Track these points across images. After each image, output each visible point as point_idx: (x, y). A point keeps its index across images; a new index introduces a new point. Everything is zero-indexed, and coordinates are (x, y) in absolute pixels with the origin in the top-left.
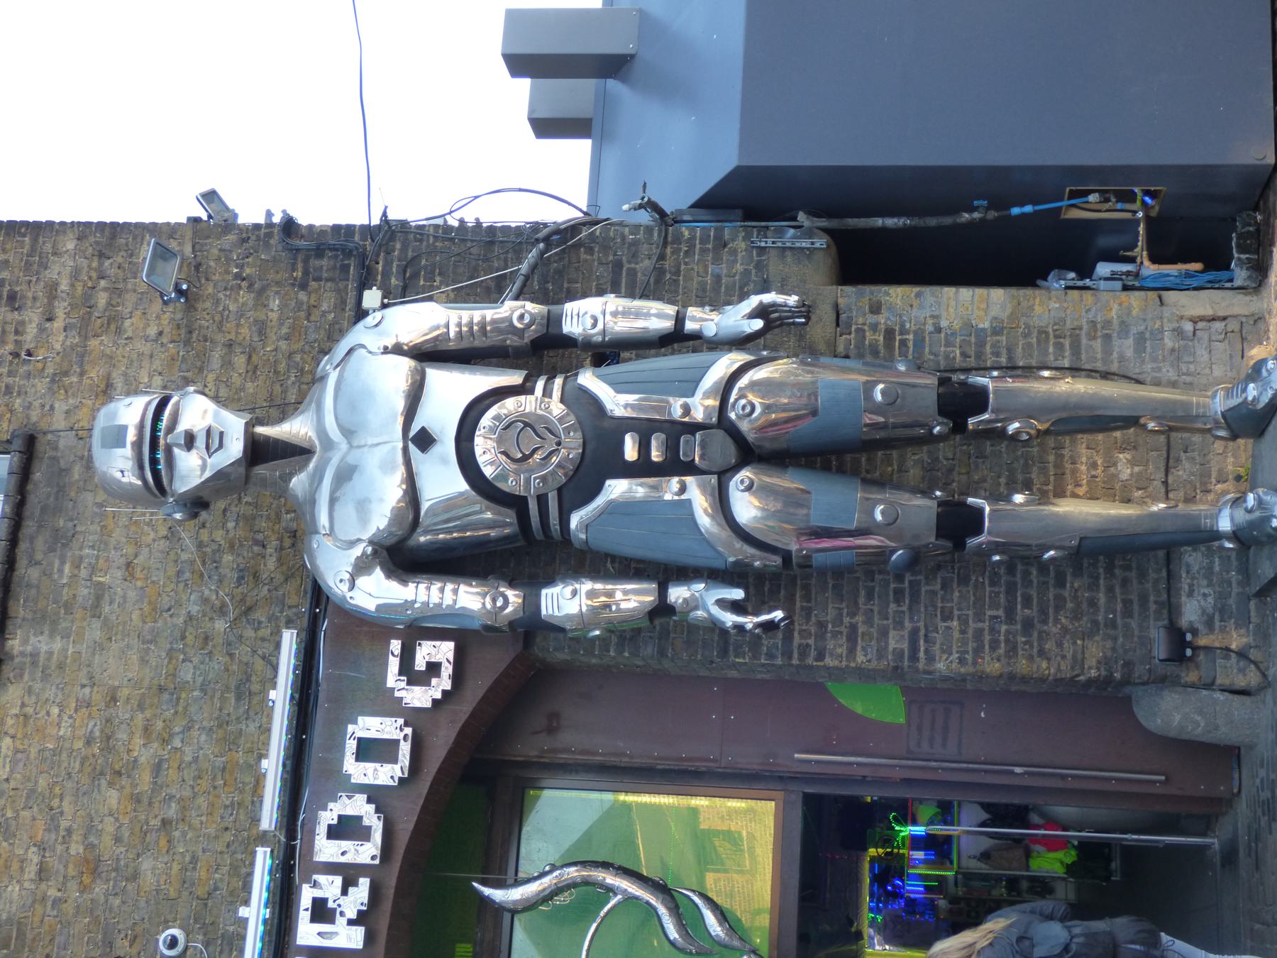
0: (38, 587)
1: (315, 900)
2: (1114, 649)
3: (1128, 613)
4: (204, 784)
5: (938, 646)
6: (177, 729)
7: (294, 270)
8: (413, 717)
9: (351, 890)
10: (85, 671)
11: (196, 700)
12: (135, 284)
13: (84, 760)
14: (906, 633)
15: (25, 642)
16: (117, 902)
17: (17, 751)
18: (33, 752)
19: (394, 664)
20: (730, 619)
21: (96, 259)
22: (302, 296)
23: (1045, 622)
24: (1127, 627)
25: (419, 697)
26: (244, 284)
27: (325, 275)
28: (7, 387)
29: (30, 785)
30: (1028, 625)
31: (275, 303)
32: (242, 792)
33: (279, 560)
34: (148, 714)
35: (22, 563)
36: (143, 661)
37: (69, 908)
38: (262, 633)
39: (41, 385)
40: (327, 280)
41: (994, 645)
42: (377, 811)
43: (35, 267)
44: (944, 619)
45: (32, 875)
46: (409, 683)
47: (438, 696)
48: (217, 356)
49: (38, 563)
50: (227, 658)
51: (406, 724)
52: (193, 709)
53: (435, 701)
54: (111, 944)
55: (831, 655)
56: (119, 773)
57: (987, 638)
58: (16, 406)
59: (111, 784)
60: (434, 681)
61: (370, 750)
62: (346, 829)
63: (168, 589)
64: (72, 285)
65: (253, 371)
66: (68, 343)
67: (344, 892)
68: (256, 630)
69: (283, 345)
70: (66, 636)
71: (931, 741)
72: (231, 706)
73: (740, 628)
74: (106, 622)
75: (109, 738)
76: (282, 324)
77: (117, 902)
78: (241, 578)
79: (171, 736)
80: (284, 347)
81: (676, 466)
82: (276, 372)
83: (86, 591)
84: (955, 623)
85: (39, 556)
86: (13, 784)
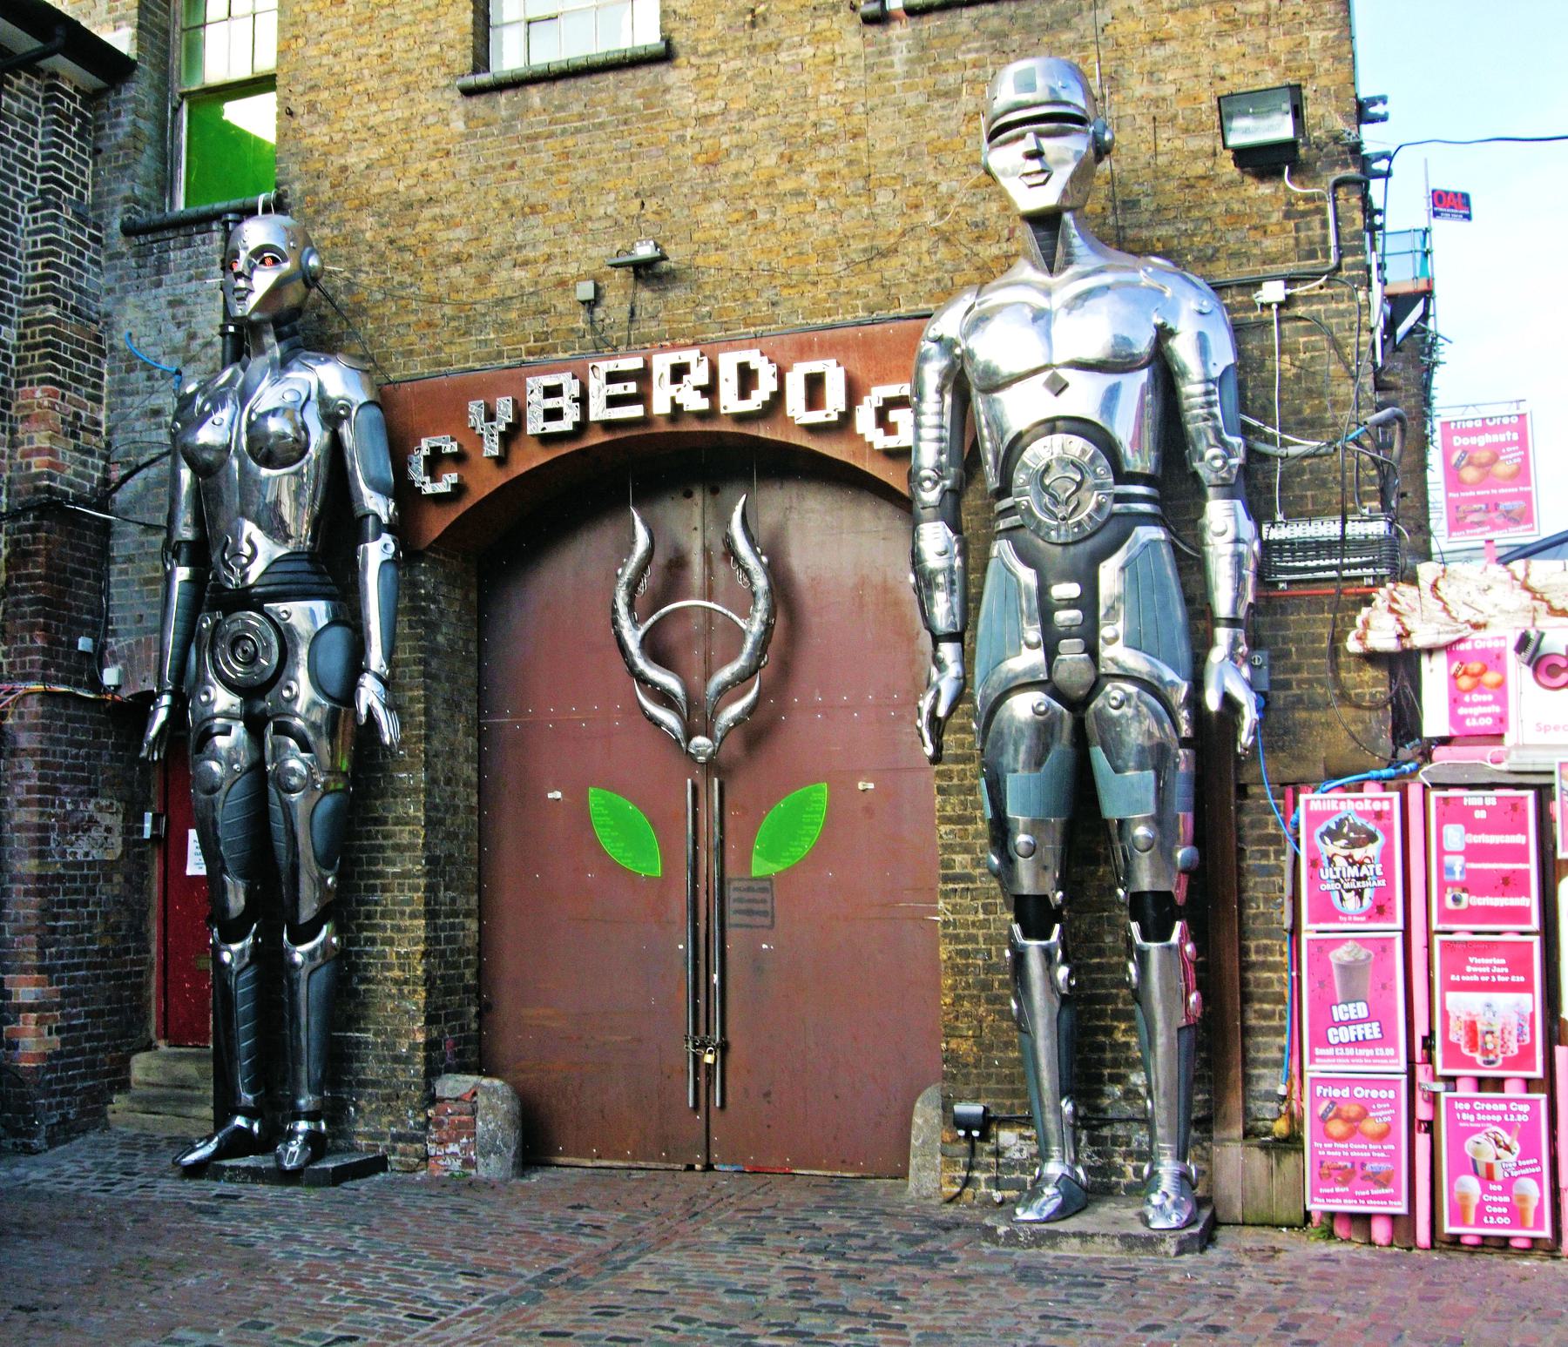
2: (966, 1065)
4: (787, 239)
8: (847, 418)
10: (877, 101)
14: (969, 870)
15: (900, 39)
16: (685, 190)
19: (893, 391)
20: (925, 704)
22: (1276, 216)
23: (989, 1001)
25: (865, 420)
27: (1302, 235)
29: (775, 84)
33: (997, 257)
34: (845, 171)
36: (891, 154)
37: (678, 150)
38: (926, 258)
40: (1297, 239)
42: (764, 403)
44: (985, 906)
45: (702, 111)
47: (867, 439)
50: (899, 230)
52: (851, 212)
54: (653, 194)
55: (944, 801)
57: (970, 947)
59: (782, 156)
61: (815, 384)
62: (747, 378)
67: (696, 388)
69: (1220, 208)
70: (908, 75)
71: (740, 900)
72: (857, 245)
73: (920, 716)
74: (923, 108)
75: (820, 142)
77: (685, 190)
79: (827, 198)
80: (1217, 211)
82: (1189, 209)
83: (951, 81)
84: (981, 916)
86: (774, 68)
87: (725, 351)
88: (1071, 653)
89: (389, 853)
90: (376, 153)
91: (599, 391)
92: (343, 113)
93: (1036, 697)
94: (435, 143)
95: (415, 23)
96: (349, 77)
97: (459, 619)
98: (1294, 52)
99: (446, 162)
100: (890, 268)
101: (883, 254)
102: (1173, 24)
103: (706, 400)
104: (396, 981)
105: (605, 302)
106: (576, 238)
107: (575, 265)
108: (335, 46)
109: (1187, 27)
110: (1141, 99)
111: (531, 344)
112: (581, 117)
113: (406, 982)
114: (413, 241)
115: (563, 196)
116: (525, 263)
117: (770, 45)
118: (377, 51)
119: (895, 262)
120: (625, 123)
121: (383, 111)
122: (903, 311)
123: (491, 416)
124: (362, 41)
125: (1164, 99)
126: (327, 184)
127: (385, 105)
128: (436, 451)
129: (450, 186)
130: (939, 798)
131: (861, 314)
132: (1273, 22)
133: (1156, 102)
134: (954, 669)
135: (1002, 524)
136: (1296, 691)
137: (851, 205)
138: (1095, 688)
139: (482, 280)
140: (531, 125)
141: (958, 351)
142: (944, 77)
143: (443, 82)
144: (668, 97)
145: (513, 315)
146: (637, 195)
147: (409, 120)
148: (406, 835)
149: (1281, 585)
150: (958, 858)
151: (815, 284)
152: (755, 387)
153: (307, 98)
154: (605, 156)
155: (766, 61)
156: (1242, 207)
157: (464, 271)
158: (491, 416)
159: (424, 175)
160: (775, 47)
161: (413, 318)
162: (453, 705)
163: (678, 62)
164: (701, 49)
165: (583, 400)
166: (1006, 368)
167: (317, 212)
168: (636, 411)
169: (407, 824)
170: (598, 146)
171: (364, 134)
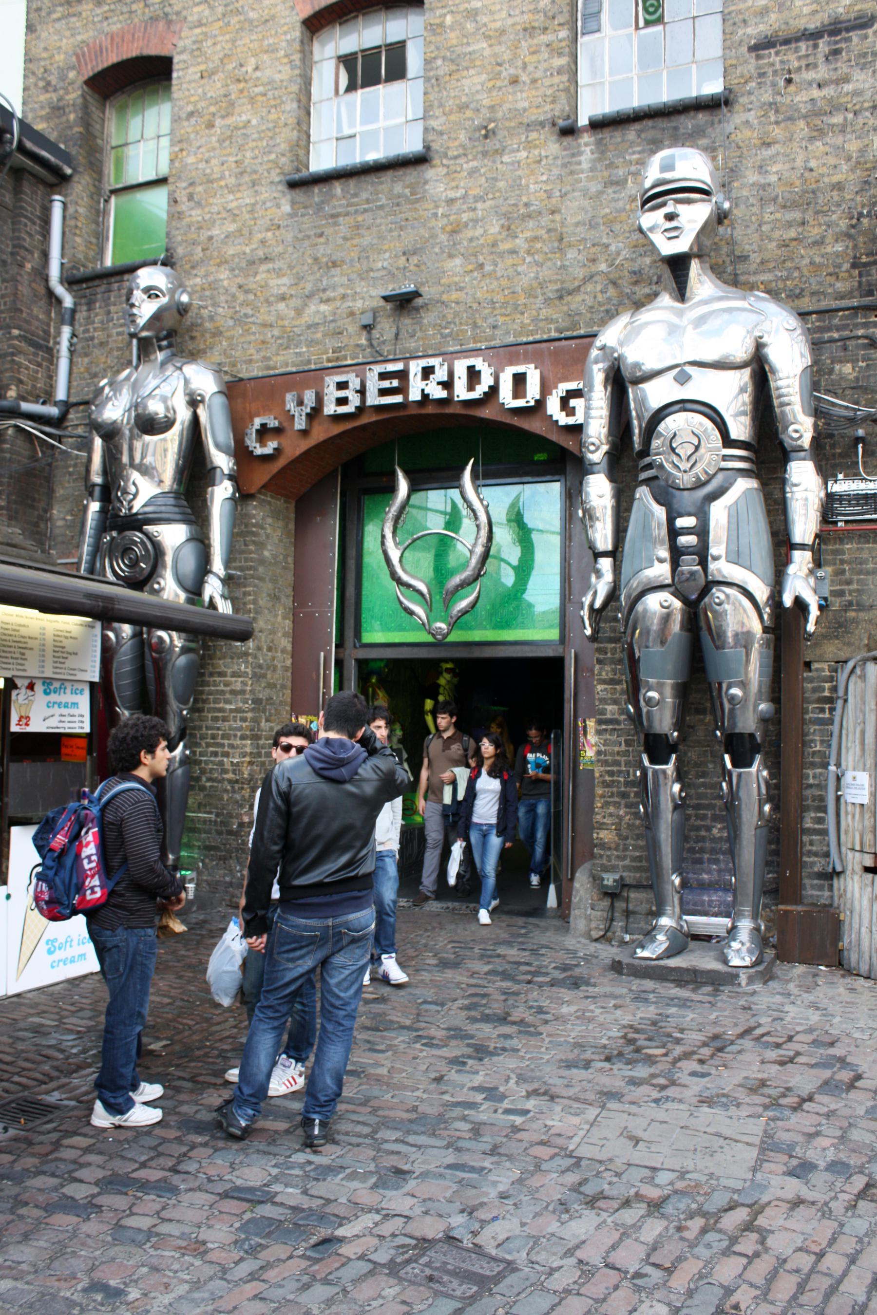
0: (623, 141)
1: (433, 367)
3: (634, 859)
4: (504, 282)
5: (608, 737)
6: (536, 257)
7: (867, 255)
8: (540, 404)
9: (440, 387)
10: (569, 188)
11: (555, 264)
12: (850, 140)
13: (515, 205)
14: (616, 716)
15: (586, 145)
17: (519, 162)
18: (519, 173)
19: (573, 385)
20: (587, 600)
21: (871, 104)
22: (846, 266)
23: (626, 806)
24: (624, 858)
25: (553, 406)
26: (854, 221)
27: (864, 279)
28: (764, 73)
29: (500, 177)
30: (624, 795)
31: (839, 247)
32: (501, 307)
34: (545, 236)
35: (637, 126)
36: (577, 224)
37: (433, 223)
38: (599, 295)
39: (767, 96)
40: (860, 283)
41: (611, 773)
42: (485, 393)
43: (863, 61)
44: (626, 741)
46: (562, 398)
47: (555, 418)
48: (796, 215)
49: (639, 136)
51: (536, 401)
52: (549, 264)
53: (551, 416)
54: (414, 253)
55: (601, 669)
56: (509, 229)
57: (615, 769)
58: (750, 84)
59: (502, 226)
60: (564, 413)
61: (519, 380)
63: (625, 227)
64: (848, 94)
65: (784, 244)
66: (801, 105)
67: (439, 383)
68: (601, 292)
69: (806, 261)
70: (592, 170)
73: (582, 608)
74: (601, 193)
75: (529, 216)
76: (823, 256)
77: (437, 250)
78: (635, 273)
80: (804, 262)
81: (676, 554)
82: (784, 261)
83: (621, 173)
85: (643, 136)
86: (499, 166)
87: (459, 358)
88: (689, 564)
89: (228, 696)
90: (232, 227)
91: (373, 385)
92: (211, 200)
93: (665, 596)
94: (271, 220)
95: (261, 139)
96: (215, 176)
97: (281, 541)
98: (862, 151)
99: (277, 233)
100: (576, 302)
101: (570, 293)
102: (777, 132)
103: (446, 392)
104: (230, 781)
105: (378, 327)
106: (363, 283)
107: (361, 301)
108: (207, 155)
109: (787, 134)
110: (753, 184)
111: (330, 355)
112: (368, 201)
113: (237, 781)
114: (254, 286)
115: (354, 255)
116: (328, 300)
117: (497, 151)
118: (234, 159)
119: (578, 298)
120: (398, 205)
121: (237, 199)
122: (582, 332)
123: (300, 403)
124: (224, 152)
125: (769, 185)
126: (200, 248)
127: (239, 195)
128: (263, 425)
129: (280, 249)
130: (597, 667)
131: (554, 335)
132: (849, 129)
133: (764, 187)
134: (608, 577)
135: (643, 476)
136: (848, 598)
137: (550, 259)
138: (706, 590)
139: (299, 312)
140: (335, 207)
141: (616, 355)
142: (615, 171)
143: (277, 179)
144: (427, 187)
145: (319, 336)
146: (404, 254)
147: (254, 205)
148: (239, 684)
149: (840, 524)
150: (609, 708)
151: (522, 313)
152: (479, 383)
153: (187, 191)
154: (383, 228)
155: (494, 162)
156: (822, 260)
157: (287, 306)
158: (300, 403)
159: (263, 242)
160: (500, 152)
161: (253, 338)
162: (275, 598)
163: (434, 162)
164: (450, 154)
165: (362, 392)
166: (650, 364)
167: (193, 267)
168: (398, 399)
169: (240, 676)
170: (378, 221)
171: (224, 215)
